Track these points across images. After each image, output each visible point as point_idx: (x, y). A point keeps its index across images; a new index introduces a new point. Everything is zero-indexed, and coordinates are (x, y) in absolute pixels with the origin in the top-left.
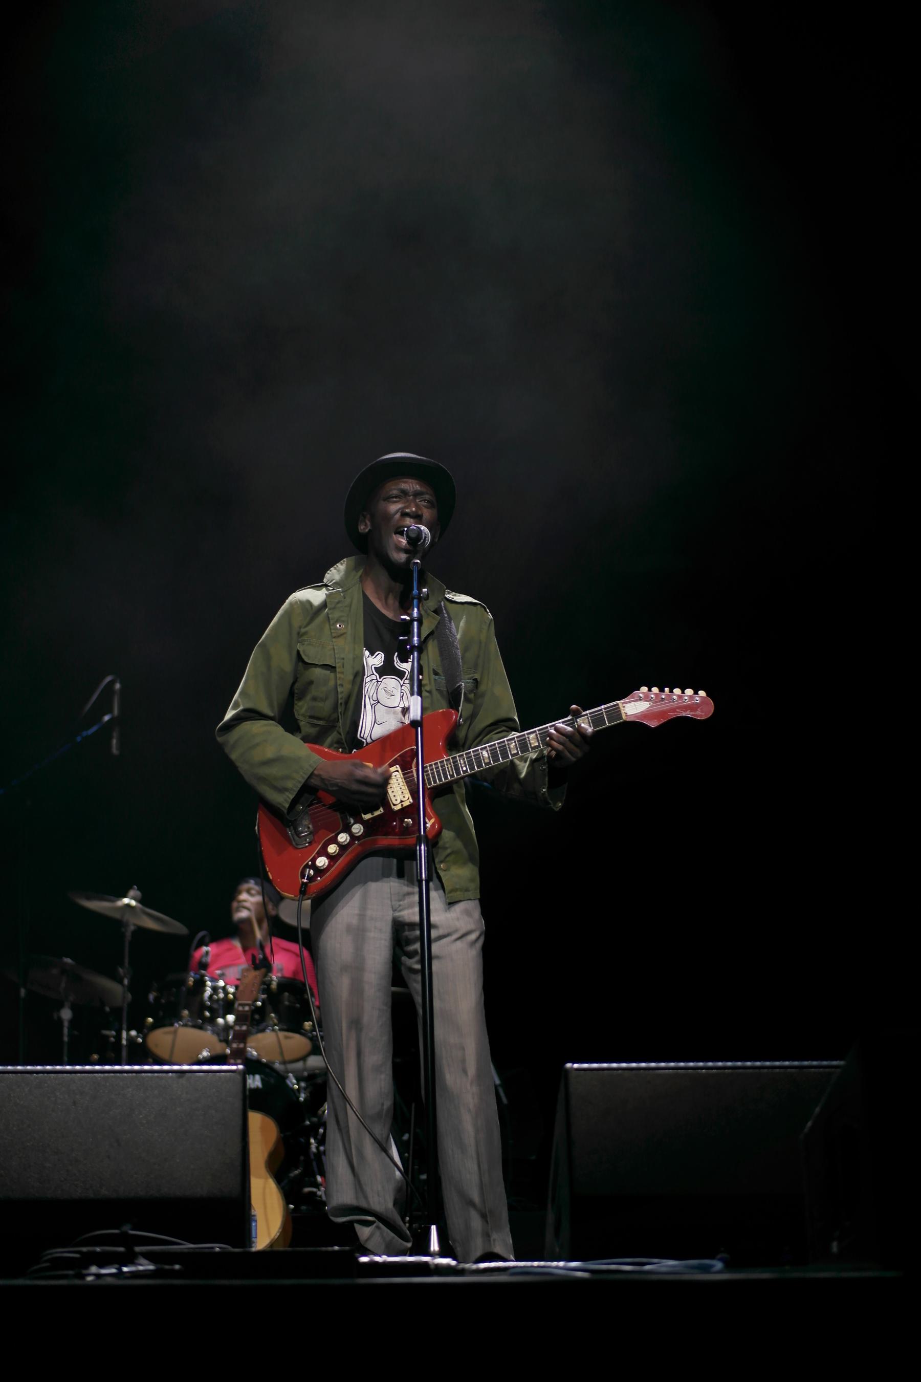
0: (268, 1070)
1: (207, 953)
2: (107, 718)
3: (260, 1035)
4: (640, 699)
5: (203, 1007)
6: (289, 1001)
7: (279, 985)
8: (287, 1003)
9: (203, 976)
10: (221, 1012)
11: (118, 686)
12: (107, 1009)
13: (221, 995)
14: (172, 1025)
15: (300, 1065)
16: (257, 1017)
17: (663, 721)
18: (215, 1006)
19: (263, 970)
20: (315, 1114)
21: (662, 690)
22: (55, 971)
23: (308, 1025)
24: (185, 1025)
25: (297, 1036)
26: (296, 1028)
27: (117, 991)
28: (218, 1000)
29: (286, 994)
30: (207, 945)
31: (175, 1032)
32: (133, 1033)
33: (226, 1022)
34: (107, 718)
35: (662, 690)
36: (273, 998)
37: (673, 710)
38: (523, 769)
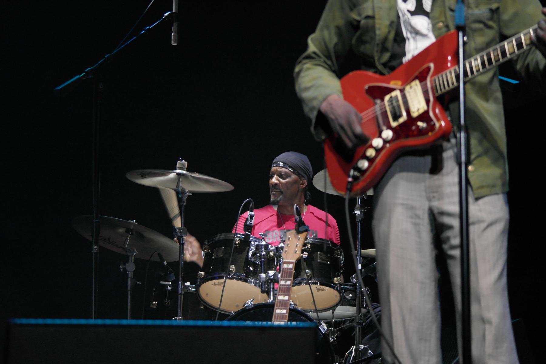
5: (248, 263)
6: (321, 259)
9: (248, 236)
12: (165, 263)
14: (221, 278)
22: (121, 230)
23: (336, 280)
24: (233, 278)
25: (327, 288)
26: (327, 282)
30: (251, 211)
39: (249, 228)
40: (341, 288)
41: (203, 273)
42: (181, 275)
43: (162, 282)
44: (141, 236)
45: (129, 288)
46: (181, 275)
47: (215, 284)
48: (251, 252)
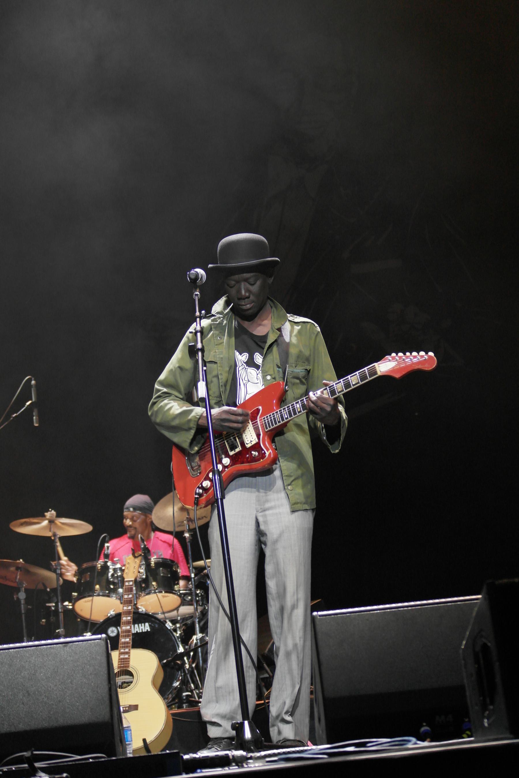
0: (153, 619)
1: (108, 547)
3: (147, 597)
5: (109, 583)
7: (155, 563)
12: (48, 590)
17: (404, 373)
18: (116, 581)
21: (405, 354)
22: (12, 569)
24: (99, 595)
25: (171, 595)
26: (170, 590)
28: (118, 577)
30: (108, 542)
31: (92, 600)
32: (66, 603)
35: (405, 354)
39: (107, 556)
40: (180, 594)
41: (76, 594)
42: (60, 598)
43: (47, 605)
44: (28, 572)
45: (23, 612)
46: (60, 598)
47: (86, 602)
48: (110, 574)
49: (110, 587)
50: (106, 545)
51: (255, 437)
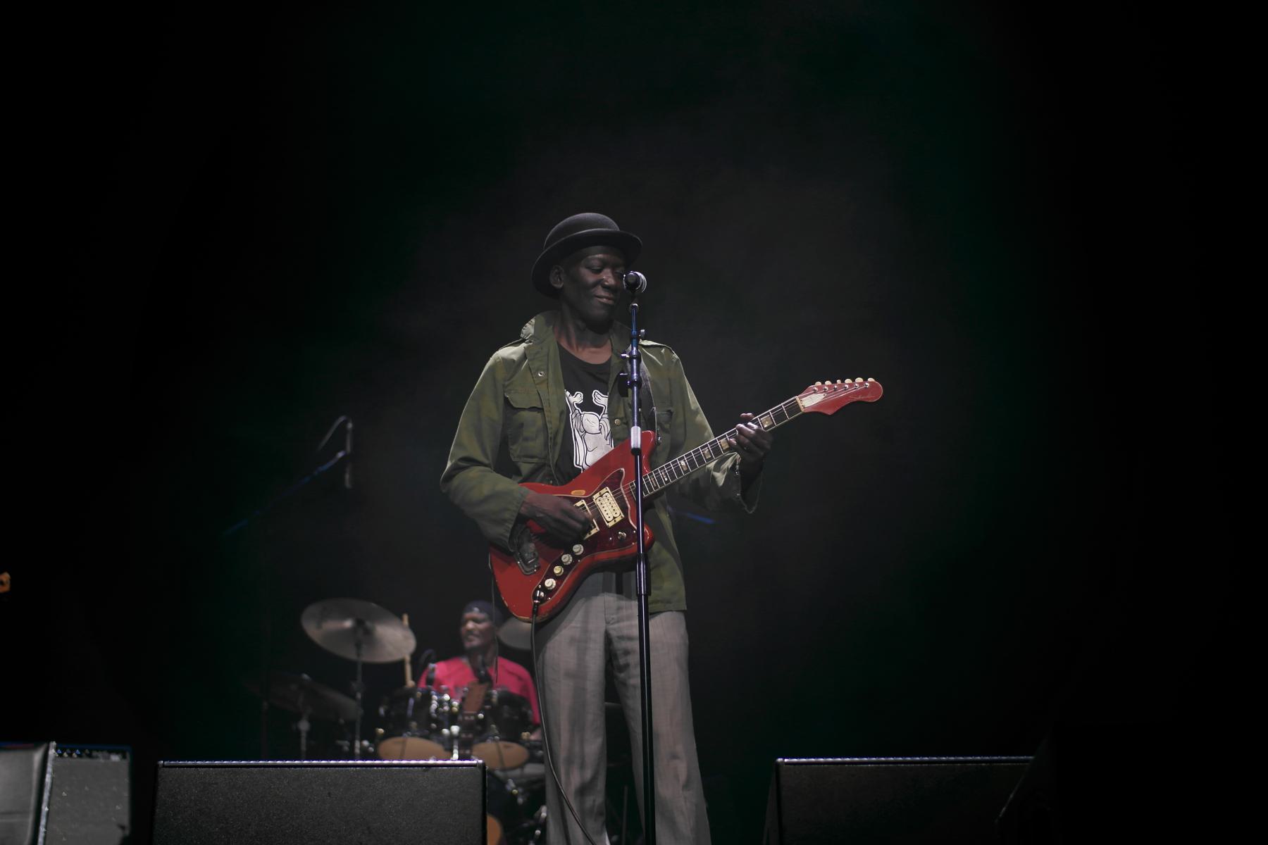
1: (433, 670)
2: (340, 455)
3: (482, 745)
4: (815, 392)
5: (430, 719)
8: (506, 715)
10: (446, 723)
11: (350, 426)
13: (446, 708)
14: (400, 735)
15: (517, 772)
16: (479, 728)
19: (487, 684)
20: (532, 817)
21: (834, 382)
23: (525, 735)
24: (413, 735)
26: (515, 738)
27: (352, 707)
29: (506, 707)
31: (404, 743)
32: (366, 743)
33: (451, 733)
34: (340, 455)
36: (493, 713)
37: (846, 397)
38: (720, 478)
39: (430, 681)
42: (358, 736)
46: (358, 736)
49: (431, 726)
50: (432, 666)
51: (619, 511)
